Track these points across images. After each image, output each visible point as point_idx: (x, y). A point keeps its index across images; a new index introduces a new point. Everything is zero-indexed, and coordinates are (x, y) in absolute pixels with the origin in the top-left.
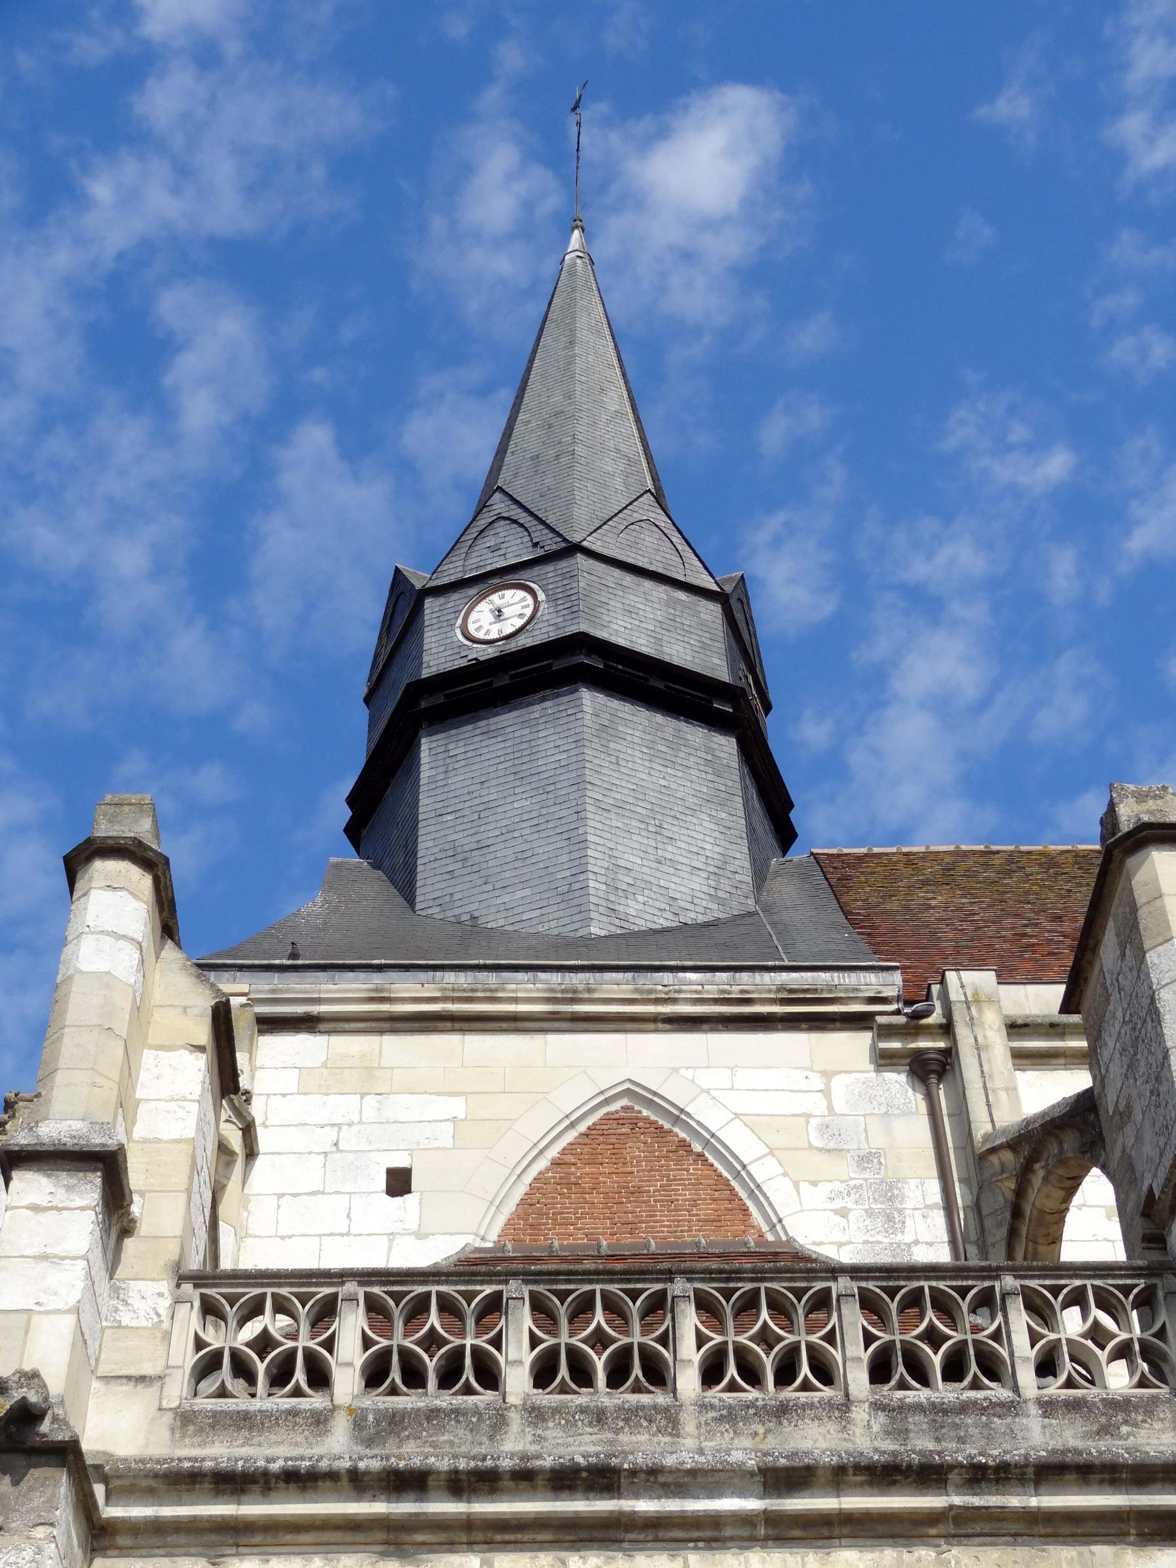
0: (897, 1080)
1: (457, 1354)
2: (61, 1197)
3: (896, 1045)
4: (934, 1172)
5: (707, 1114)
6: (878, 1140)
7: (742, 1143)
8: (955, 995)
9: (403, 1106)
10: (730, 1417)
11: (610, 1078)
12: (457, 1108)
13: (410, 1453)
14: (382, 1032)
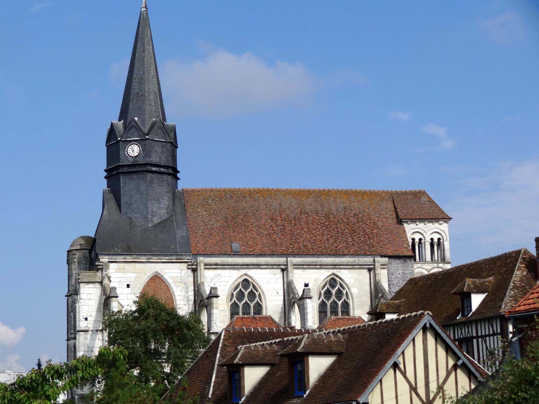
0: (190, 271)
3: (190, 267)
4: (193, 285)
5: (166, 277)
6: (187, 281)
7: (170, 281)
8: (198, 261)
9: (129, 275)
11: (154, 271)
12: (134, 275)
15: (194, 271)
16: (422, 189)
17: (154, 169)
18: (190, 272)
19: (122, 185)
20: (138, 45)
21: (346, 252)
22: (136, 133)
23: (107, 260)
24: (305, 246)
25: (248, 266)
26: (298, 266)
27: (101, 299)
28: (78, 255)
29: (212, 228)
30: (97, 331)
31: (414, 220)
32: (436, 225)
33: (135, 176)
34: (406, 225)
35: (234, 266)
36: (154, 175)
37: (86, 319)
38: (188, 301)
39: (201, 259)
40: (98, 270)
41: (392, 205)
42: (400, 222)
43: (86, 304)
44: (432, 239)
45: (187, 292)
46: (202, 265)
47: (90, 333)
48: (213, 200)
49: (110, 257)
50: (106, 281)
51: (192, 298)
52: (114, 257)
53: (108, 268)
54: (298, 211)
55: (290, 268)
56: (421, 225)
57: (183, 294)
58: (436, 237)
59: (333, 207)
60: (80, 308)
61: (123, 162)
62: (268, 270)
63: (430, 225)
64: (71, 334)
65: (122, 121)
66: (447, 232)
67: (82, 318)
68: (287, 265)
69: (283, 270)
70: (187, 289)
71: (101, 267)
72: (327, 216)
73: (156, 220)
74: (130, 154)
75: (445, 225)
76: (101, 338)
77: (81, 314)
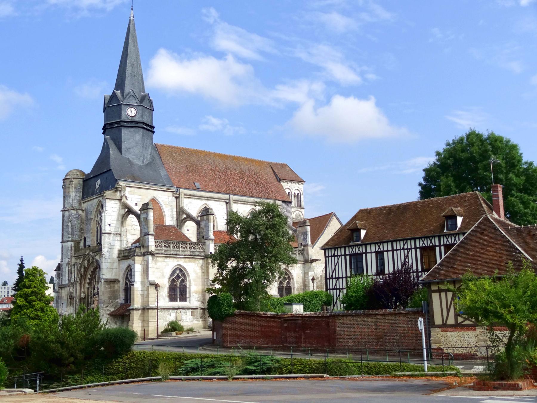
0: (174, 198)
9: (136, 196)
10: (183, 251)
11: (152, 196)
12: (140, 197)
13: (167, 253)
15: (176, 198)
16: (285, 163)
17: (145, 127)
18: (174, 199)
19: (122, 134)
20: (130, 41)
21: (257, 195)
22: (134, 100)
23: (124, 185)
24: (235, 190)
25: (208, 198)
26: (236, 201)
27: (119, 211)
28: (75, 182)
29: (180, 172)
30: (117, 234)
31: (287, 180)
32: (297, 184)
33: (132, 129)
34: (282, 183)
35: (200, 198)
36: (145, 131)
37: (110, 225)
38: (173, 218)
39: (182, 190)
40: (117, 191)
41: (271, 170)
42: (279, 180)
44: (295, 193)
45: (172, 212)
46: (183, 194)
47: (112, 235)
48: (175, 153)
49: (126, 183)
50: (124, 199)
51: (175, 216)
52: (129, 183)
53: (125, 190)
54: (224, 167)
55: (231, 202)
56: (290, 184)
57: (170, 213)
58: (297, 192)
59: (242, 167)
60: (106, 217)
61: (124, 118)
62: (218, 202)
63: (294, 184)
64: (69, 238)
65: (119, 91)
66: (302, 190)
67: (107, 224)
68: (230, 200)
69: (227, 203)
70: (172, 210)
72: (241, 172)
73: (146, 162)
75: (302, 185)
76: (119, 239)
77: (107, 221)
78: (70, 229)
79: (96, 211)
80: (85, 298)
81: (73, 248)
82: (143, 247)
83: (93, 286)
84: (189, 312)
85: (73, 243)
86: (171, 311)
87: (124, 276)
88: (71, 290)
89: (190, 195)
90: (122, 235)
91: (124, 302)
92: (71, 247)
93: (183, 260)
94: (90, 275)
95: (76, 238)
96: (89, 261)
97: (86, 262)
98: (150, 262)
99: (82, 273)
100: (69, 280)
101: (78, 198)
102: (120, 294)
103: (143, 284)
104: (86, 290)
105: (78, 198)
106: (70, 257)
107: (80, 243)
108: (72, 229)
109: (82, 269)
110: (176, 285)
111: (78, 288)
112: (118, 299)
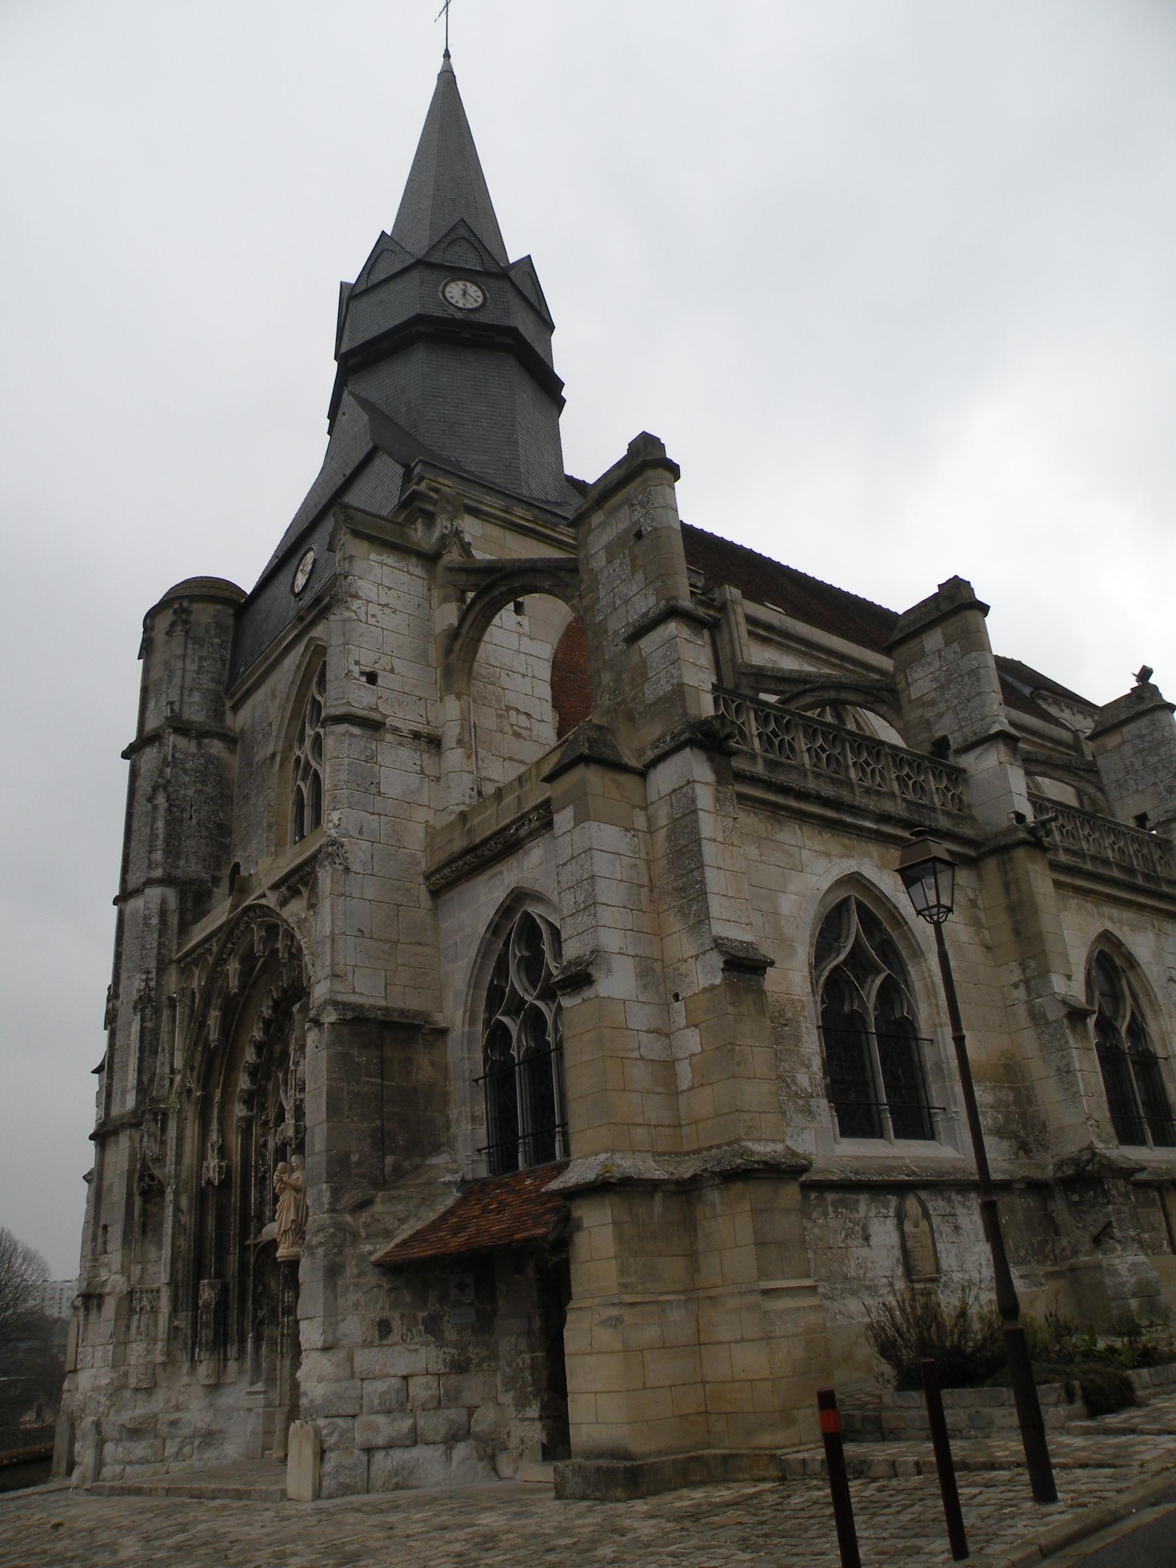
1: (782, 742)
2: (693, 638)
10: (868, 791)
13: (781, 778)
14: (504, 528)
30: (416, 736)
37: (372, 678)
43: (372, 621)
71: (430, 508)
74: (453, 301)
77: (355, 654)
78: (160, 824)
79: (296, 713)
80: (225, 1184)
81: (173, 920)
82: (630, 717)
83: (272, 1113)
84: (971, 1219)
85: (171, 895)
86: (864, 1205)
87: (474, 983)
88: (151, 1148)
89: (770, 627)
90: (450, 741)
91: (483, 1172)
92: (163, 913)
93: (873, 849)
94: (259, 1047)
95: (191, 868)
96: (248, 959)
97: (233, 967)
98: (705, 797)
99: (214, 1036)
100: (142, 1089)
101: (211, 686)
102: (453, 1113)
103: (656, 975)
104: (235, 1142)
105: (211, 686)
106: (152, 965)
107: (209, 894)
108: (173, 824)
109: (214, 1015)
110: (857, 1018)
111: (192, 1129)
112: (436, 1149)
